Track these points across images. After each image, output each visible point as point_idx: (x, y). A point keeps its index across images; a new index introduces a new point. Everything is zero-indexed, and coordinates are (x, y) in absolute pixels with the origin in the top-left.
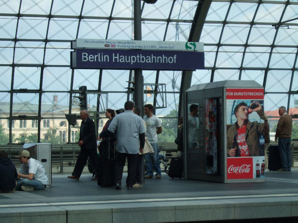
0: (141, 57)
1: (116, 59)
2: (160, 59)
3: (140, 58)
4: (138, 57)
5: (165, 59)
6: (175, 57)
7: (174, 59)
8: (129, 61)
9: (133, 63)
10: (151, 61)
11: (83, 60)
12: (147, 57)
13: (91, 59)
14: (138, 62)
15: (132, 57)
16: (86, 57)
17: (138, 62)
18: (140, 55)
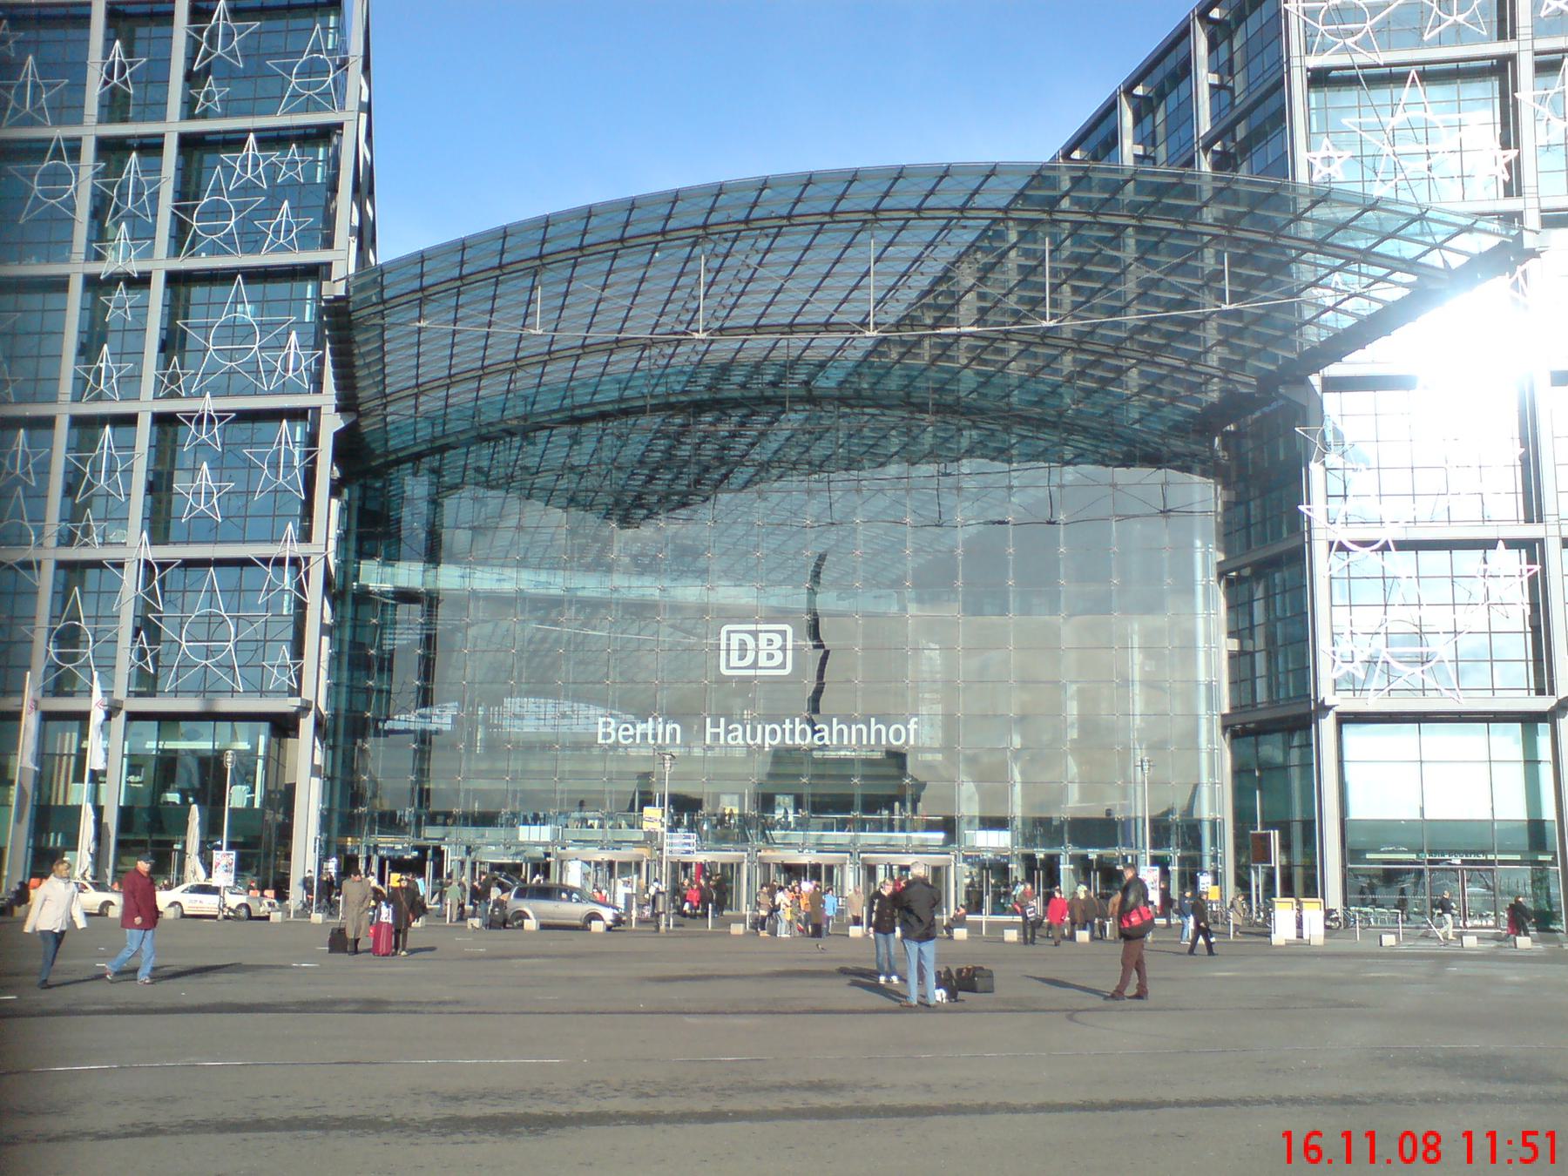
0: (798, 728)
1: (716, 736)
2: (860, 731)
3: (792, 732)
4: (787, 726)
5: (878, 732)
7: (907, 730)
8: (759, 741)
9: (770, 745)
10: (831, 739)
11: (600, 741)
12: (816, 728)
13: (626, 738)
14: (788, 742)
15: (768, 728)
18: (793, 722)
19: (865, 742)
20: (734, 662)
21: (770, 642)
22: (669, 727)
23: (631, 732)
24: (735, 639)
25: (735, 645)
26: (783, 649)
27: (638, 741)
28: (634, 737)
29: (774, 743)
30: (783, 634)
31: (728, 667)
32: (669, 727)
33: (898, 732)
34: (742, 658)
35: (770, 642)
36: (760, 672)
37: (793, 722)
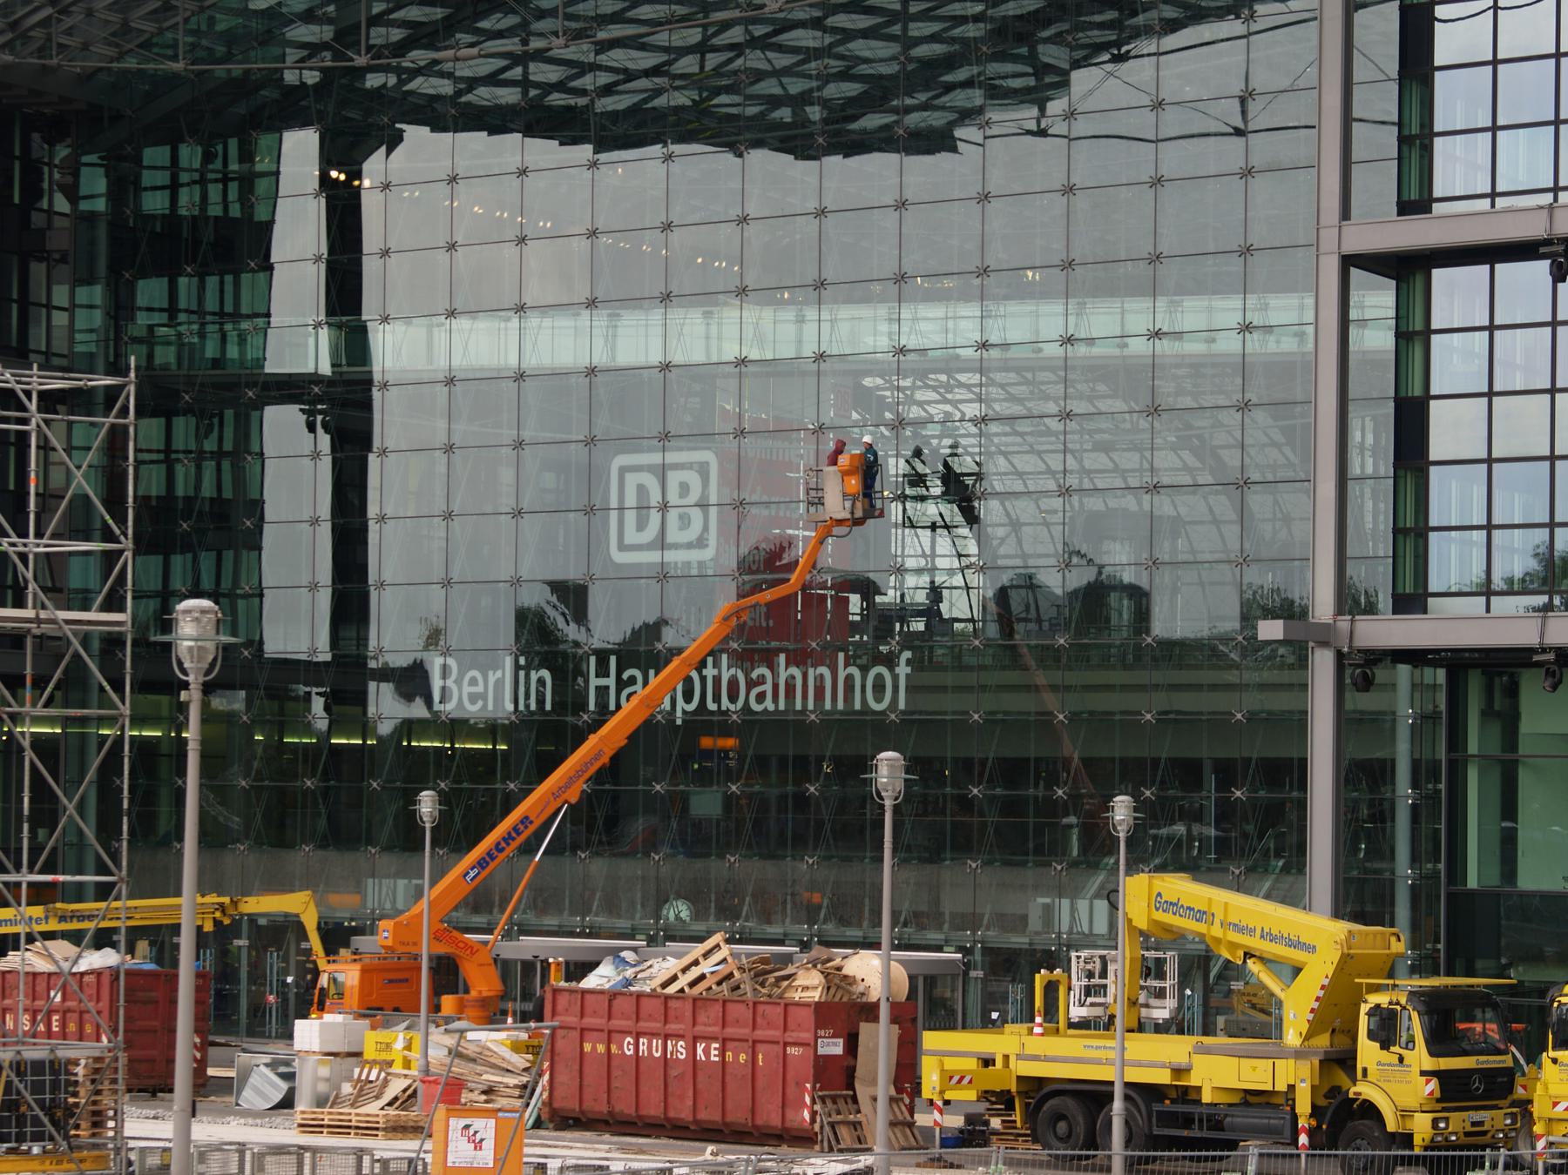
3: (717, 680)
4: (710, 672)
5: (849, 679)
6: (903, 670)
7: (895, 678)
9: (684, 712)
12: (754, 675)
13: (473, 698)
16: (450, 683)
17: (712, 706)
18: (716, 665)
19: (828, 706)
20: (632, 536)
21: (684, 489)
22: (534, 676)
23: (480, 689)
24: (632, 480)
25: (631, 500)
26: (703, 505)
27: (490, 707)
28: (484, 696)
29: (692, 707)
30: (703, 470)
31: (622, 547)
32: (534, 676)
33: (879, 679)
34: (641, 526)
35: (684, 489)
36: (671, 556)
37: (716, 665)
